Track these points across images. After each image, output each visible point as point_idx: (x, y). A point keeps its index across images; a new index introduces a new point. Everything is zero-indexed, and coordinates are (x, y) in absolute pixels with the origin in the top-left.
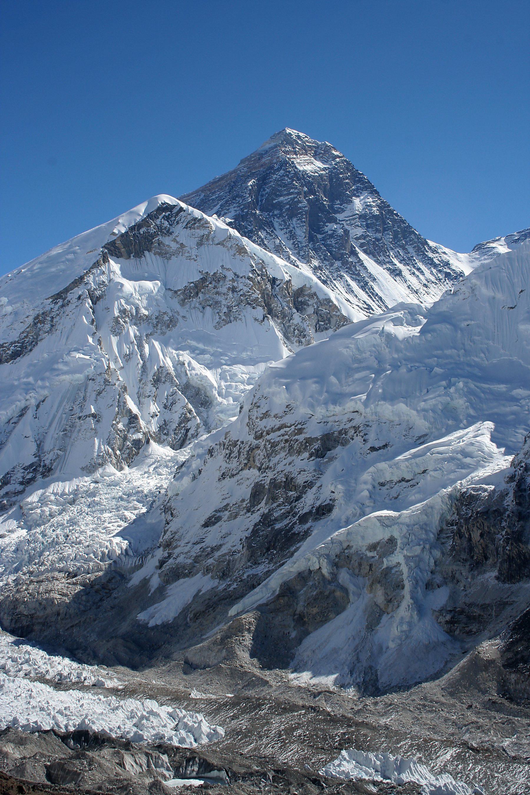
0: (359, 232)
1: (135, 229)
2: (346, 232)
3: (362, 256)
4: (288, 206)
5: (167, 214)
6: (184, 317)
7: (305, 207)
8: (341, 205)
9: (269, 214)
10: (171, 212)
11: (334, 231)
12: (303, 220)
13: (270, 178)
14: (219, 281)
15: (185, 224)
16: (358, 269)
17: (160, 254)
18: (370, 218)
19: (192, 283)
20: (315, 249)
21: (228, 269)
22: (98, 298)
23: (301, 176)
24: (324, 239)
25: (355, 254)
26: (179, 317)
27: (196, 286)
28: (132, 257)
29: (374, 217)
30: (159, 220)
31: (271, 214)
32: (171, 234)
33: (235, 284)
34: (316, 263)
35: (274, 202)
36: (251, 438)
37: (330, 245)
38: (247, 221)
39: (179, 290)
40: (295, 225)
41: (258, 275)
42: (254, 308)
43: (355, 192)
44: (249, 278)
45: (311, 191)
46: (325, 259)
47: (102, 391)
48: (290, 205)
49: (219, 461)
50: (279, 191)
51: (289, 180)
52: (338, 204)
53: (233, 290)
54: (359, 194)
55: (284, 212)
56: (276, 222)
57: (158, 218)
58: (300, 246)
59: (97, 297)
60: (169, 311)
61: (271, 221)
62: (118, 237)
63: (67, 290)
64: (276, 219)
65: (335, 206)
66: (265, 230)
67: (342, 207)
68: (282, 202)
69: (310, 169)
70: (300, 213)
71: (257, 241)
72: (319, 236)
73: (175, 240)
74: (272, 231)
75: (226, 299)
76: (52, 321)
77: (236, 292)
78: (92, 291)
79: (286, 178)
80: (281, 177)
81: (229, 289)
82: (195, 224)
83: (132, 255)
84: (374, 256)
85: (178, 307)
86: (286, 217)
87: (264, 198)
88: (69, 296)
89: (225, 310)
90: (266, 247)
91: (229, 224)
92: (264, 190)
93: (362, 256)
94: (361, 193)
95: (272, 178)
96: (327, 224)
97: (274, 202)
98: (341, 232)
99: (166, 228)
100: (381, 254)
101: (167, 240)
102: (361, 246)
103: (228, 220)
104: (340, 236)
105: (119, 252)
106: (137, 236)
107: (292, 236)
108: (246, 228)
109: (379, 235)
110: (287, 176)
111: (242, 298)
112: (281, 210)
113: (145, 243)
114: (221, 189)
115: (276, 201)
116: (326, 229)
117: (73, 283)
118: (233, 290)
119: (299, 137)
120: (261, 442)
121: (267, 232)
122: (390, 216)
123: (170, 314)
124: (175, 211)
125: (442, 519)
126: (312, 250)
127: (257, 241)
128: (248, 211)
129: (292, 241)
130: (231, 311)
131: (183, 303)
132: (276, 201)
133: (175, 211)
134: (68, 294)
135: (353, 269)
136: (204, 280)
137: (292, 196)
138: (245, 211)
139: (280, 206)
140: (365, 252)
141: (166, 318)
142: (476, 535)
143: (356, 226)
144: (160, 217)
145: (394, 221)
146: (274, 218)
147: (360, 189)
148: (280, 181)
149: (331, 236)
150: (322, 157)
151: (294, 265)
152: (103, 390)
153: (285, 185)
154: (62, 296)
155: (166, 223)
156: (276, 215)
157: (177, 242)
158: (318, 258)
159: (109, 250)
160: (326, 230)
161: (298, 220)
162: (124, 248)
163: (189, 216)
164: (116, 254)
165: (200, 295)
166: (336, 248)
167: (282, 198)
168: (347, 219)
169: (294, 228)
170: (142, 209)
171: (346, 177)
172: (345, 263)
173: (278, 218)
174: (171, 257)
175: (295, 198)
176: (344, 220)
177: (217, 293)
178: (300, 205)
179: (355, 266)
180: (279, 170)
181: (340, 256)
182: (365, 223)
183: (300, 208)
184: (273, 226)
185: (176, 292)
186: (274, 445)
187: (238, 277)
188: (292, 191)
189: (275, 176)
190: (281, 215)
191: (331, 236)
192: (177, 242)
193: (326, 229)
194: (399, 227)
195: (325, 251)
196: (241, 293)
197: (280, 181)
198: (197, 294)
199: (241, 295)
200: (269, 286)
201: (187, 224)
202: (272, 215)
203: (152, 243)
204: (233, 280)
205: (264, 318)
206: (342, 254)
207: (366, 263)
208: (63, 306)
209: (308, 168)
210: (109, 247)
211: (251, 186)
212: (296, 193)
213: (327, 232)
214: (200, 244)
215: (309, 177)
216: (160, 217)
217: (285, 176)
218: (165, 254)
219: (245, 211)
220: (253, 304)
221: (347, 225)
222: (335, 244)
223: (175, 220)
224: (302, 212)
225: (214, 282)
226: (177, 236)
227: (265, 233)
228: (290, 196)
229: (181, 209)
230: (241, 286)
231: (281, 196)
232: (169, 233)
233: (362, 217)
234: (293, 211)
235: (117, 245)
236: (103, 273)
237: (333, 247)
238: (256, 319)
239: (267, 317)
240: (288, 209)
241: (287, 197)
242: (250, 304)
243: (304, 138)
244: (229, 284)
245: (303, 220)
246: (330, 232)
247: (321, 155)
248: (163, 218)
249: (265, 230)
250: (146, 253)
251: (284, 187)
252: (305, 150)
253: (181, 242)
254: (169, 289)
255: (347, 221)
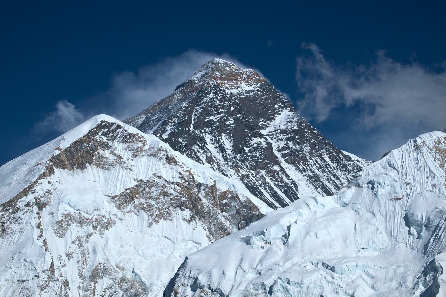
0: (282, 144)
1: (77, 144)
2: (270, 145)
3: (284, 165)
4: (217, 124)
5: (106, 131)
6: (121, 219)
7: (232, 124)
8: (265, 122)
9: (201, 131)
10: (109, 129)
11: (258, 144)
12: (231, 135)
13: (201, 101)
14: (152, 187)
15: (122, 138)
16: (280, 176)
17: (98, 165)
18: (290, 133)
19: (128, 189)
20: (242, 161)
21: (160, 177)
22: (44, 205)
24: (250, 151)
25: (279, 164)
26: (116, 220)
27: (132, 192)
28: (75, 169)
29: (294, 131)
30: (98, 136)
31: (203, 131)
32: (109, 148)
33: (165, 190)
34: (243, 172)
35: (206, 121)
37: (256, 156)
38: (182, 137)
39: (116, 196)
40: (224, 140)
41: (186, 181)
42: (182, 210)
43: (277, 111)
44: (178, 184)
45: (239, 111)
46: (251, 169)
47: (46, 286)
48: (219, 123)
50: (209, 111)
51: (218, 102)
52: (262, 121)
53: (165, 194)
54: (280, 112)
55: (214, 129)
56: (208, 138)
57: (98, 134)
58: (229, 157)
59: (43, 204)
60: (107, 214)
61: (203, 137)
62: (62, 152)
63: (17, 198)
64: (208, 136)
65: (260, 123)
66: (198, 145)
67: (266, 124)
68: (212, 120)
69: (237, 92)
70: (227, 130)
71: (191, 155)
72: (246, 149)
73: (112, 153)
74: (204, 146)
75: (158, 203)
76: (3, 226)
77: (167, 196)
78: (39, 199)
79: (216, 100)
80: (211, 99)
81: (160, 194)
82: (130, 138)
83: (75, 167)
84: (295, 165)
85: (116, 210)
86: (216, 134)
87: (197, 117)
88: (19, 204)
89: (157, 212)
90: (198, 160)
91: (166, 141)
92: (197, 111)
93: (284, 165)
94: (282, 111)
95: (203, 100)
96: (252, 139)
97: (206, 121)
98: (264, 144)
99: (105, 142)
100: (301, 163)
101: (106, 153)
102: (284, 156)
103: (165, 136)
104: (264, 149)
105: (63, 165)
106: (80, 150)
107: (222, 149)
108: (181, 143)
109: (298, 147)
110: (217, 98)
111: (172, 201)
112: (212, 127)
113: (86, 156)
114: (160, 112)
115: (207, 120)
116: (252, 143)
117: (22, 192)
118: (165, 194)
119: (227, 65)
121: (199, 146)
122: (307, 130)
123: (108, 217)
124: (113, 127)
126: (240, 161)
127: (191, 155)
128: (182, 129)
129: (221, 154)
130: (162, 213)
131: (119, 207)
132: (207, 120)
133: (113, 127)
134: (18, 202)
135: (276, 176)
137: (221, 115)
138: (180, 128)
139: (210, 124)
140: (287, 161)
141: (105, 220)
143: (278, 139)
144: (100, 133)
145: (312, 134)
146: (206, 134)
147: (282, 108)
148: (210, 102)
149: (256, 149)
150: (247, 82)
151: (224, 174)
152: (47, 285)
153: (215, 106)
154: (12, 204)
155: (105, 139)
156: (207, 132)
157: (115, 155)
158: (245, 168)
159: (55, 163)
160: (252, 144)
161: (226, 135)
162: (68, 160)
163: (125, 133)
164: (61, 166)
165: (136, 200)
166: (261, 159)
167: (212, 118)
168: (270, 134)
169: (223, 142)
170: (86, 127)
172: (269, 172)
173: (209, 134)
174: (109, 168)
175: (223, 117)
176: (268, 135)
177: (150, 198)
178: (228, 123)
179: (278, 174)
180: (209, 93)
181: (264, 165)
182: (286, 137)
183: (229, 125)
184: (205, 141)
185: (113, 198)
187: (169, 183)
188: (221, 110)
189: (206, 98)
190: (211, 132)
191: (256, 149)
192: (115, 155)
193: (252, 143)
194: (316, 139)
195: (251, 161)
196: (172, 197)
197: (210, 102)
198: (133, 199)
199: (171, 199)
200: (196, 190)
201: (123, 139)
202: (204, 132)
203: (93, 156)
204: (164, 186)
205: (191, 219)
206: (267, 164)
207: (287, 171)
208: (14, 212)
209: (235, 91)
210: (54, 160)
211: (184, 107)
212: (225, 113)
213: (253, 145)
214: (134, 156)
215: (236, 99)
216: (100, 133)
217: (214, 98)
218: (104, 166)
219: (180, 128)
220: (181, 205)
221: (271, 139)
222: (260, 155)
223: (112, 136)
224: (230, 129)
225: (147, 189)
226: (115, 150)
227: (197, 147)
228: (219, 116)
229: (119, 127)
230: (172, 191)
231: (211, 115)
232: (107, 147)
234: (222, 128)
235: (61, 158)
236: (49, 183)
237: (258, 158)
238: (184, 219)
239: (194, 217)
240: (218, 127)
241: (217, 116)
242: (178, 206)
243: (231, 66)
244: (160, 190)
245: (231, 135)
246: (255, 146)
247: (246, 80)
248: (102, 134)
249: (198, 145)
250: (87, 165)
251: (214, 107)
252: (233, 76)
253: (118, 154)
254: (108, 195)
255: (271, 135)
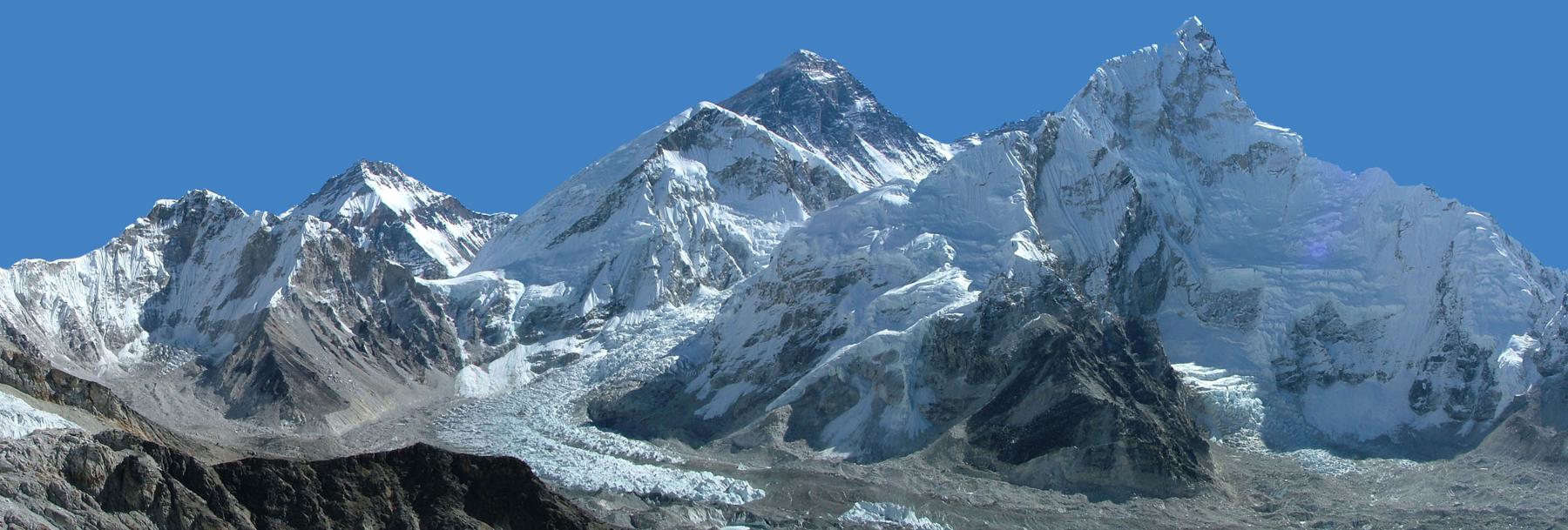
0: (861, 125)
3: (864, 143)
23: (814, 85)
25: (857, 141)
36: (780, 280)
45: (822, 95)
49: (755, 298)
93: (864, 143)
107: (807, 129)
120: (789, 283)
125: (925, 337)
131: (722, 182)
136: (738, 164)
139: (797, 107)
142: (951, 350)
171: (849, 85)
186: (798, 285)
209: (818, 78)
220: (779, 180)
232: (710, 130)
233: (863, 114)
234: (809, 110)
252: (816, 65)
